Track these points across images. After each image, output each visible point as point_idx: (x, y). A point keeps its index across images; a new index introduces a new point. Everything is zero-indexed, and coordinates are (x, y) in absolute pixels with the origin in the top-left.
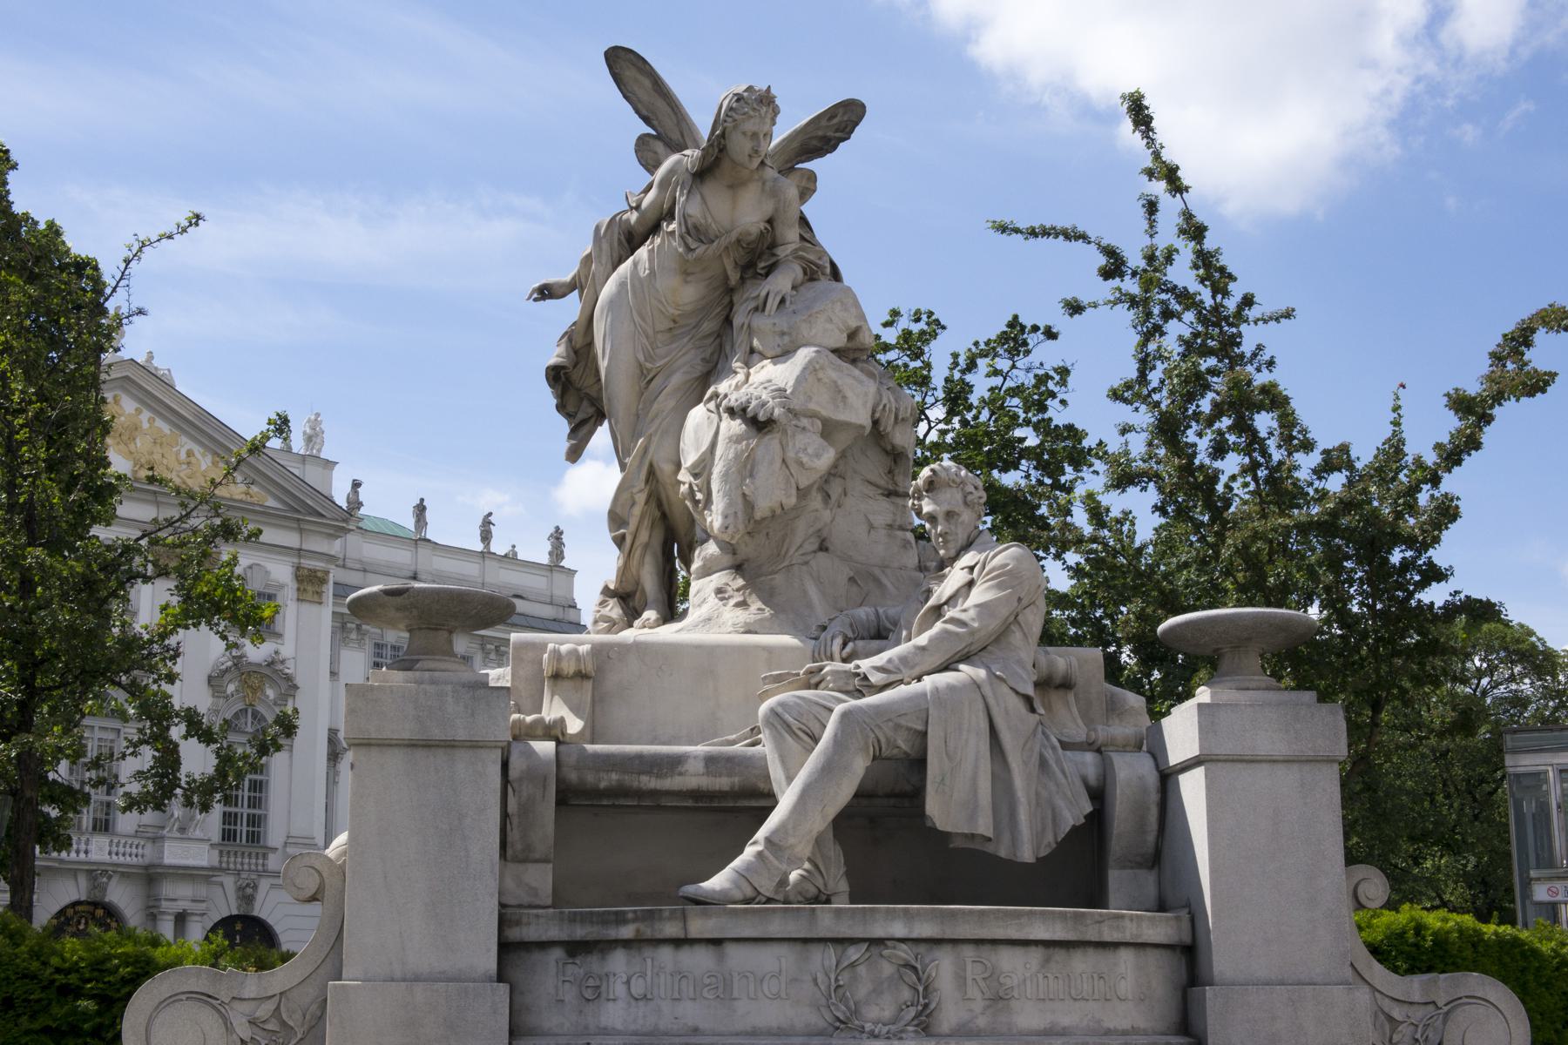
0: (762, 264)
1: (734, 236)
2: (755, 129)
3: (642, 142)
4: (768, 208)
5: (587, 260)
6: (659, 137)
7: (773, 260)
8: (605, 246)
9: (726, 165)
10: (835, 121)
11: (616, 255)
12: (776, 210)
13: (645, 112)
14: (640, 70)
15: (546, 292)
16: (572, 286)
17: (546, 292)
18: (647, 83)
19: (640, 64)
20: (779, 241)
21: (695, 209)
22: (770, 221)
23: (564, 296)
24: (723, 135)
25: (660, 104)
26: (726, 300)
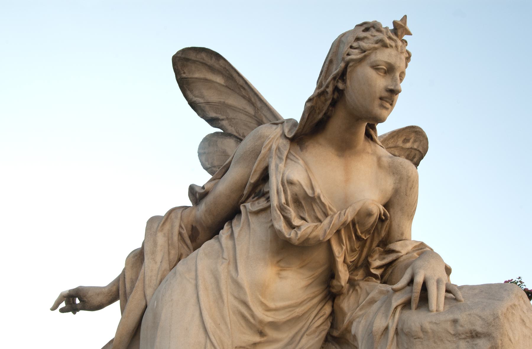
0: (377, 263)
1: (349, 215)
2: (392, 61)
3: (209, 140)
4: (389, 184)
5: (138, 258)
6: (226, 134)
7: (390, 258)
8: (161, 239)
9: (337, 124)
10: (408, 145)
11: (174, 253)
12: (396, 192)
13: (213, 115)
14: (211, 69)
15: (76, 301)
16: (116, 293)
17: (76, 301)
18: (219, 79)
19: (212, 62)
20: (396, 234)
21: (297, 173)
22: (387, 206)
23: (99, 307)
24: (342, 75)
25: (234, 100)
26: (327, 310)
